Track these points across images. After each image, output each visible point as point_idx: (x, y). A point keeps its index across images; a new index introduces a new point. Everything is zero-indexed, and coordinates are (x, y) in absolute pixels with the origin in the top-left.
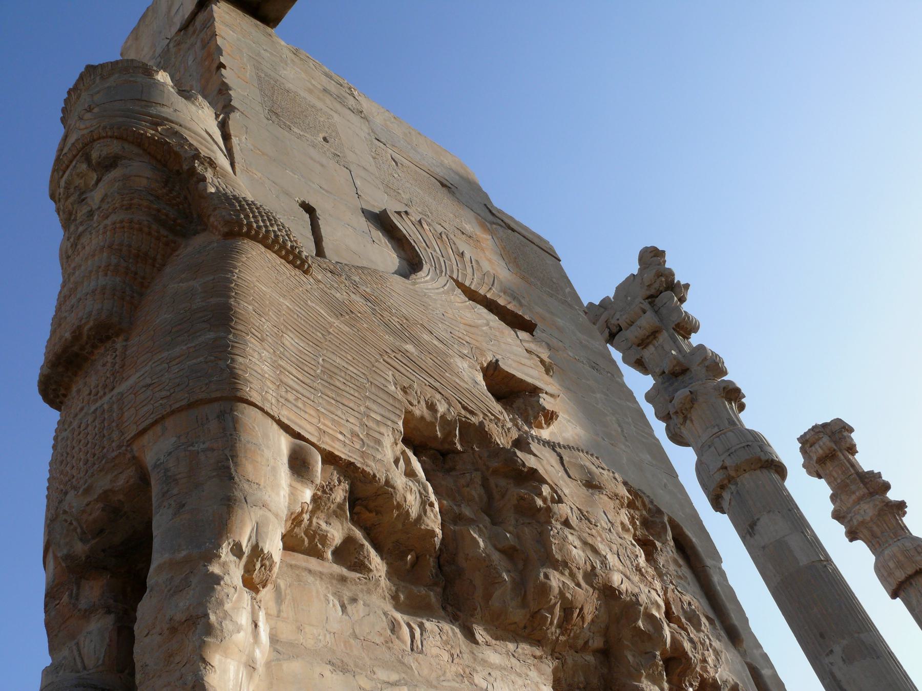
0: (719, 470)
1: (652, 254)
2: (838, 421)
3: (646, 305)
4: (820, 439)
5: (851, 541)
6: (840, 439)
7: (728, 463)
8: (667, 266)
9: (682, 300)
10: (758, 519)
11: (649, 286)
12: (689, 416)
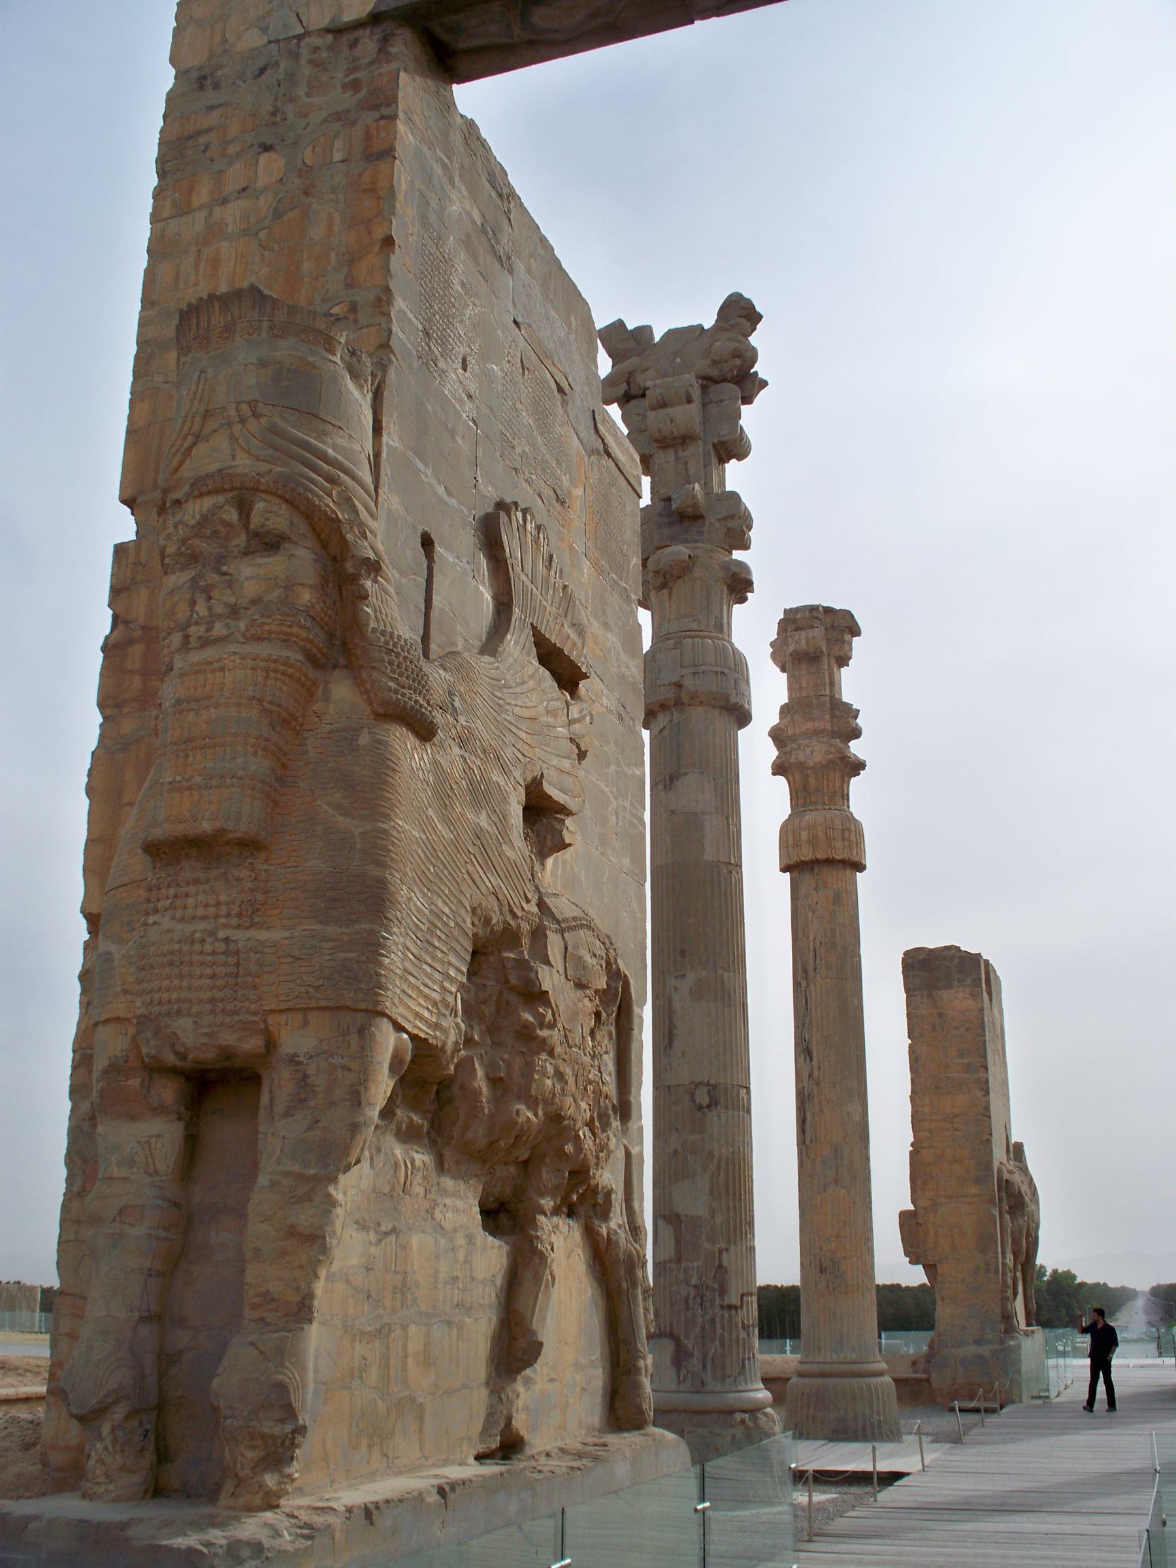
0: (669, 684)
1: (744, 312)
2: (848, 615)
3: (696, 393)
4: (812, 627)
5: (774, 774)
7: (688, 683)
8: (753, 340)
9: (747, 400)
10: (685, 774)
11: (714, 362)
12: (671, 584)
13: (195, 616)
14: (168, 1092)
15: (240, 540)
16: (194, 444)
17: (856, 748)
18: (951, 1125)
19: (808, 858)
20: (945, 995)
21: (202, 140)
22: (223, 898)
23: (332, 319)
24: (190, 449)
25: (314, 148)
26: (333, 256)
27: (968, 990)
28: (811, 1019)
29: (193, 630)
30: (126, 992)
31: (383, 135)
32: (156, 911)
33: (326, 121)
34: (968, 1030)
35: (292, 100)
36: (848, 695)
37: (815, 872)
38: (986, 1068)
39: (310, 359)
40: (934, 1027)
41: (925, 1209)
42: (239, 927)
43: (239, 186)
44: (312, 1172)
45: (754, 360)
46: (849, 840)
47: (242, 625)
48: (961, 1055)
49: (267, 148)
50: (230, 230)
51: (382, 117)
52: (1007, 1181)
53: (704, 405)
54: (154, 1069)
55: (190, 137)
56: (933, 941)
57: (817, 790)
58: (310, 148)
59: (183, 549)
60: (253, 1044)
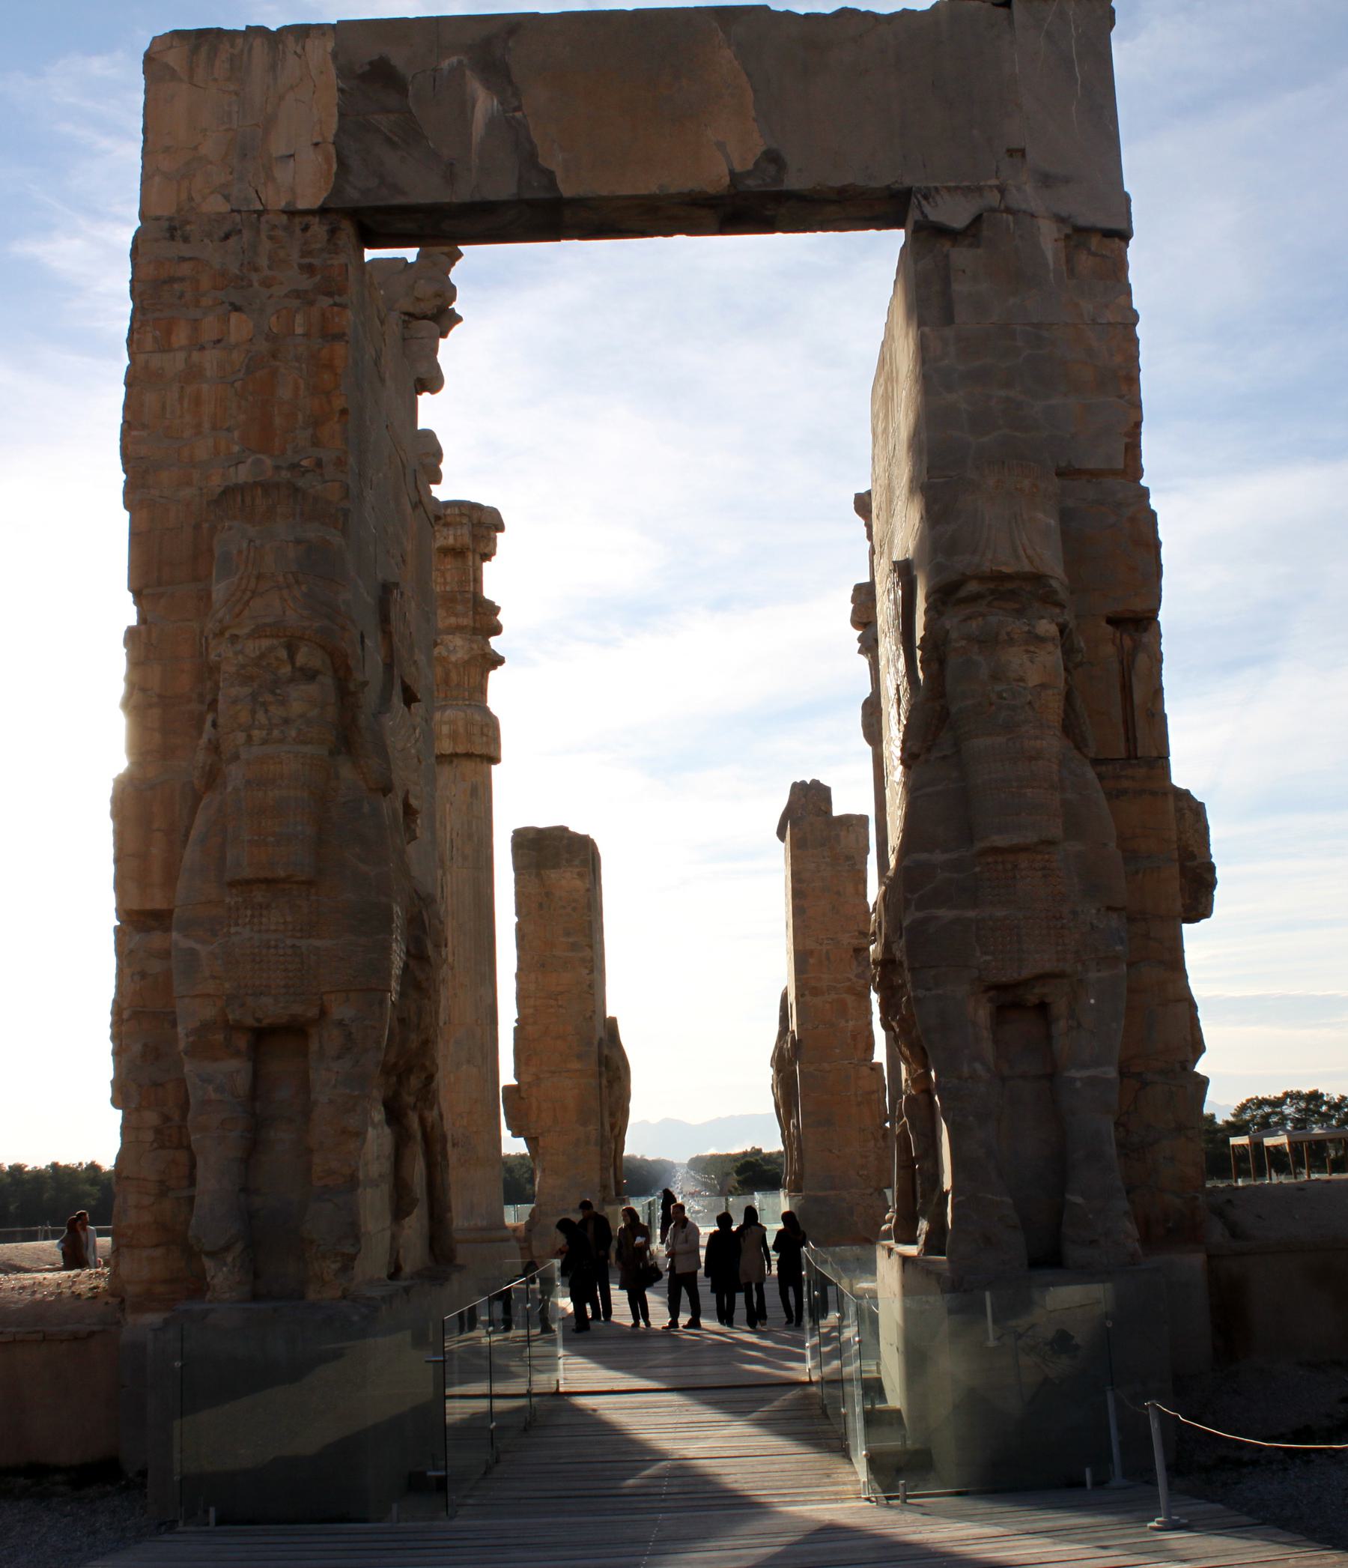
2: (494, 513)
6: (482, 537)
13: (257, 723)
14: (242, 1042)
15: (286, 670)
16: (251, 598)
17: (495, 643)
18: (553, 1002)
19: (448, 752)
20: (553, 875)
21: (176, 286)
22: (289, 919)
23: (302, 469)
24: (248, 601)
25: (278, 318)
26: (300, 417)
27: (577, 870)
28: (446, 907)
29: (256, 733)
30: (214, 977)
31: (337, 320)
32: (237, 925)
33: (286, 296)
34: (574, 909)
35: (256, 270)
36: (489, 592)
37: (454, 766)
38: (591, 947)
39: (328, 538)
40: (541, 906)
41: (529, 1083)
42: (302, 937)
43: (216, 339)
44: (356, 1093)
45: (453, 299)
46: (487, 736)
47: (293, 733)
48: (568, 934)
49: (237, 309)
50: (208, 373)
51: (335, 304)
52: (606, 1056)
53: (404, 339)
54: (232, 1028)
55: (164, 282)
56: (543, 821)
57: (458, 685)
58: (275, 316)
59: (243, 672)
60: (313, 1012)
